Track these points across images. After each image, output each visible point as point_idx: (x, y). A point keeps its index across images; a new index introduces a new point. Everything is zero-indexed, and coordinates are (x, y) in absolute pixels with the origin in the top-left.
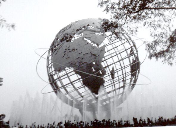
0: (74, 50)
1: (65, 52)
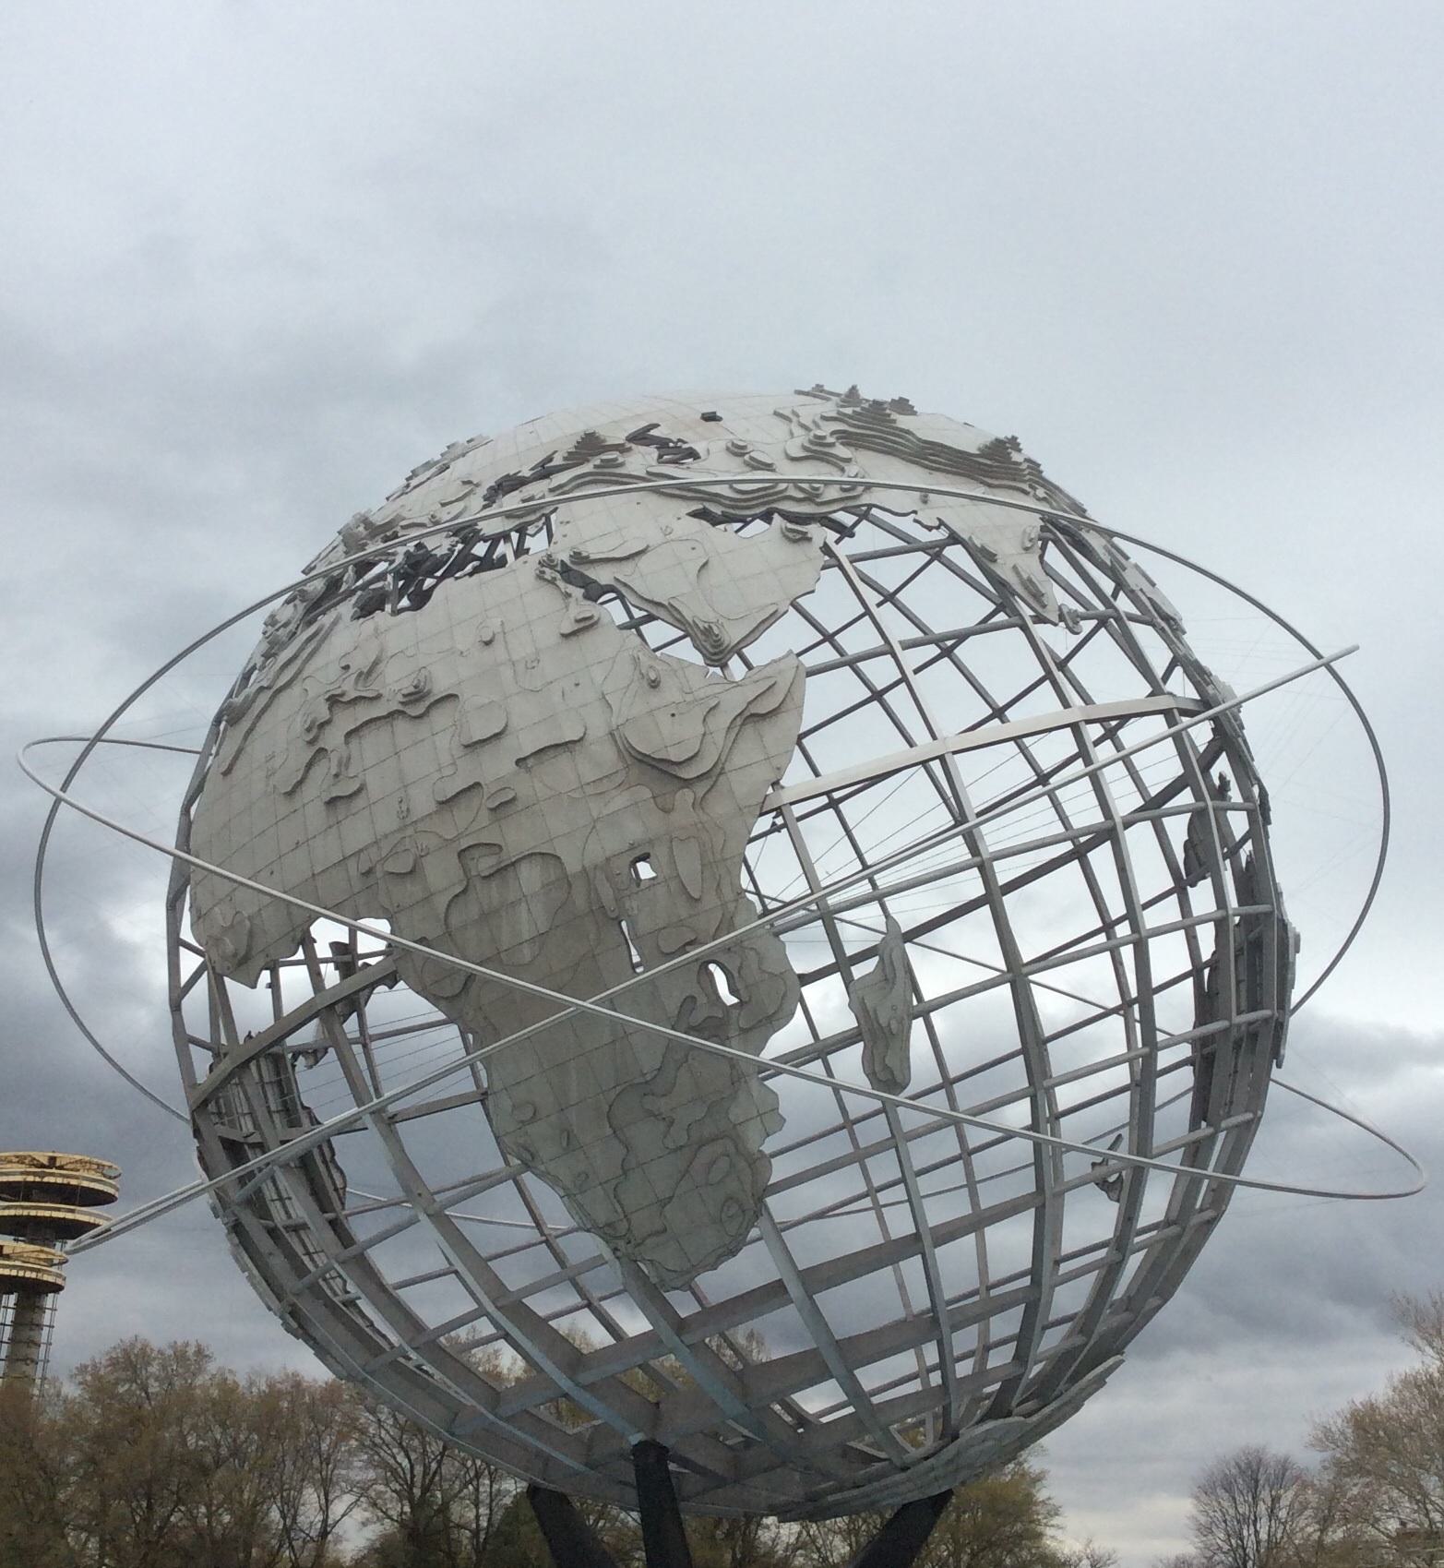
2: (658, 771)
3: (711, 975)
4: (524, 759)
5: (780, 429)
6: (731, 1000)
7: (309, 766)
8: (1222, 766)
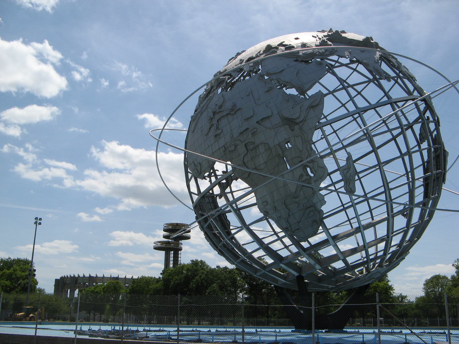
0: (233, 112)
1: (212, 119)
2: (290, 122)
4: (258, 121)
5: (314, 39)
6: (312, 175)
7: (210, 128)
8: (428, 114)
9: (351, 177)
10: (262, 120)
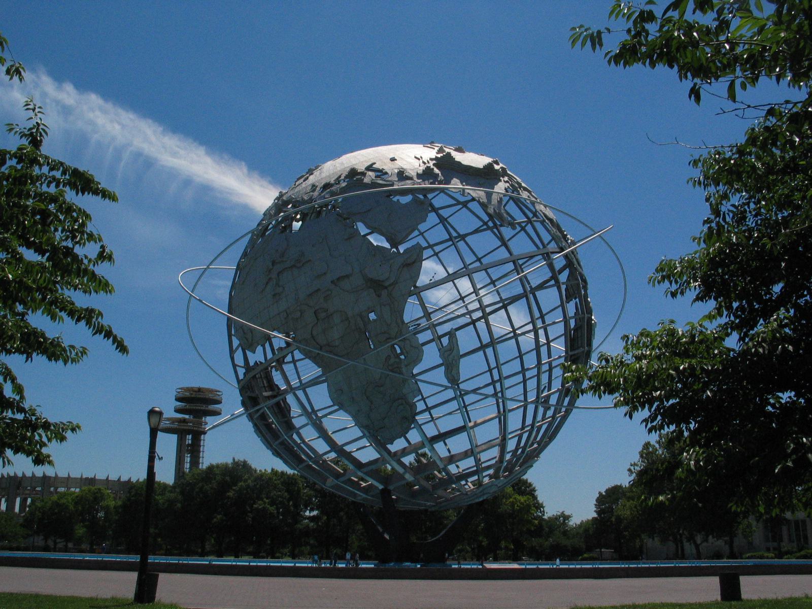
2: (376, 285)
3: (395, 349)
5: (416, 163)
9: (454, 361)
10: (338, 279)
